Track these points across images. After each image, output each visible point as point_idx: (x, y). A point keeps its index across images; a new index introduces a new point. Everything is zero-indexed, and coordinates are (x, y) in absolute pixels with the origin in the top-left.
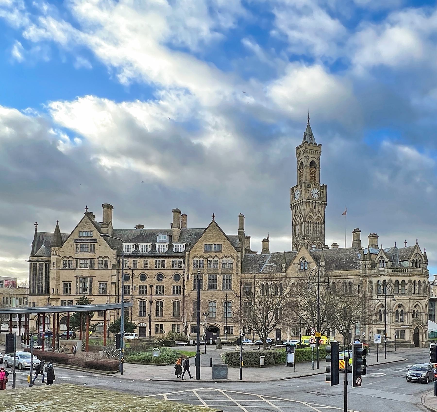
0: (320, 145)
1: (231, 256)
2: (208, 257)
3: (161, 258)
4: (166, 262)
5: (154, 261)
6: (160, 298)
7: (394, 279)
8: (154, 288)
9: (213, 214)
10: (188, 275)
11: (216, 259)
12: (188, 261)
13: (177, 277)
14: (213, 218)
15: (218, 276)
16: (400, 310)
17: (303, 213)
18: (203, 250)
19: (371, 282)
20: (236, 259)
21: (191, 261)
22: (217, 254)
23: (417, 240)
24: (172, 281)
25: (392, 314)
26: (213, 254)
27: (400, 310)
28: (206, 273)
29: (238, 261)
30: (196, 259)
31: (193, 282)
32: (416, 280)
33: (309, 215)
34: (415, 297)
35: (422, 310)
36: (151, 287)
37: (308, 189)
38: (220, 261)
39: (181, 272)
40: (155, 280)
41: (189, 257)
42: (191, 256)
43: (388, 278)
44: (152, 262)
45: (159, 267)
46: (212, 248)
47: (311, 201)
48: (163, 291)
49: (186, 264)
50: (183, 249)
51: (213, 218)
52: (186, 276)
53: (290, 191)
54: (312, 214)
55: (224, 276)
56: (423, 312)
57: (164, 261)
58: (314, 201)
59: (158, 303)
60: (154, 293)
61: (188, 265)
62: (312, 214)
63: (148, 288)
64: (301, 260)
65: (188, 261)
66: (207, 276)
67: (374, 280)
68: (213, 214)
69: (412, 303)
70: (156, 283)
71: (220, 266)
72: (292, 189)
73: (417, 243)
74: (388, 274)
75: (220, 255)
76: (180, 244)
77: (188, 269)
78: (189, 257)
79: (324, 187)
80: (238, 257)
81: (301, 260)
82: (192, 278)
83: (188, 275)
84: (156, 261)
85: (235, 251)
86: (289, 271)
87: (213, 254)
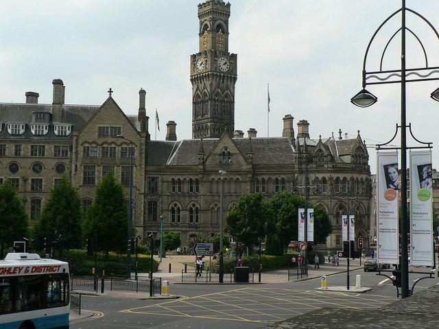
1: (132, 143)
2: (104, 143)
3: (38, 143)
4: (46, 148)
5: (30, 146)
6: (37, 195)
7: (335, 176)
8: (30, 181)
9: (110, 89)
10: (76, 166)
11: (113, 146)
12: (77, 148)
13: (60, 168)
14: (110, 94)
15: (116, 167)
17: (209, 89)
18: (97, 133)
19: (307, 179)
21: (81, 149)
22: (113, 140)
23: (359, 132)
24: (54, 172)
26: (110, 140)
28: (99, 164)
30: (87, 145)
31: (82, 175)
36: (25, 181)
38: (118, 149)
39: (66, 162)
40: (30, 172)
41: (77, 144)
42: (80, 142)
43: (327, 176)
44: (26, 149)
45: (36, 154)
46: (107, 132)
47: (218, 74)
48: (41, 187)
49: (74, 151)
50: (68, 132)
51: (110, 94)
52: (74, 167)
53: (188, 62)
54: (220, 91)
55: (123, 167)
57: (44, 147)
58: (222, 74)
59: (33, 201)
60: (29, 188)
61: (77, 153)
62: (220, 91)
63: (20, 181)
64: (223, 150)
65: (77, 148)
66: (101, 167)
67: (312, 177)
68: (110, 89)
70: (32, 176)
71: (118, 154)
72: (194, 57)
73: (359, 135)
74: (329, 172)
75: (120, 141)
76: (64, 125)
77: (77, 158)
78: (77, 144)
80: (141, 144)
81: (223, 150)
82: (81, 169)
83: (76, 166)
84: (32, 146)
86: (207, 163)
87: (110, 140)
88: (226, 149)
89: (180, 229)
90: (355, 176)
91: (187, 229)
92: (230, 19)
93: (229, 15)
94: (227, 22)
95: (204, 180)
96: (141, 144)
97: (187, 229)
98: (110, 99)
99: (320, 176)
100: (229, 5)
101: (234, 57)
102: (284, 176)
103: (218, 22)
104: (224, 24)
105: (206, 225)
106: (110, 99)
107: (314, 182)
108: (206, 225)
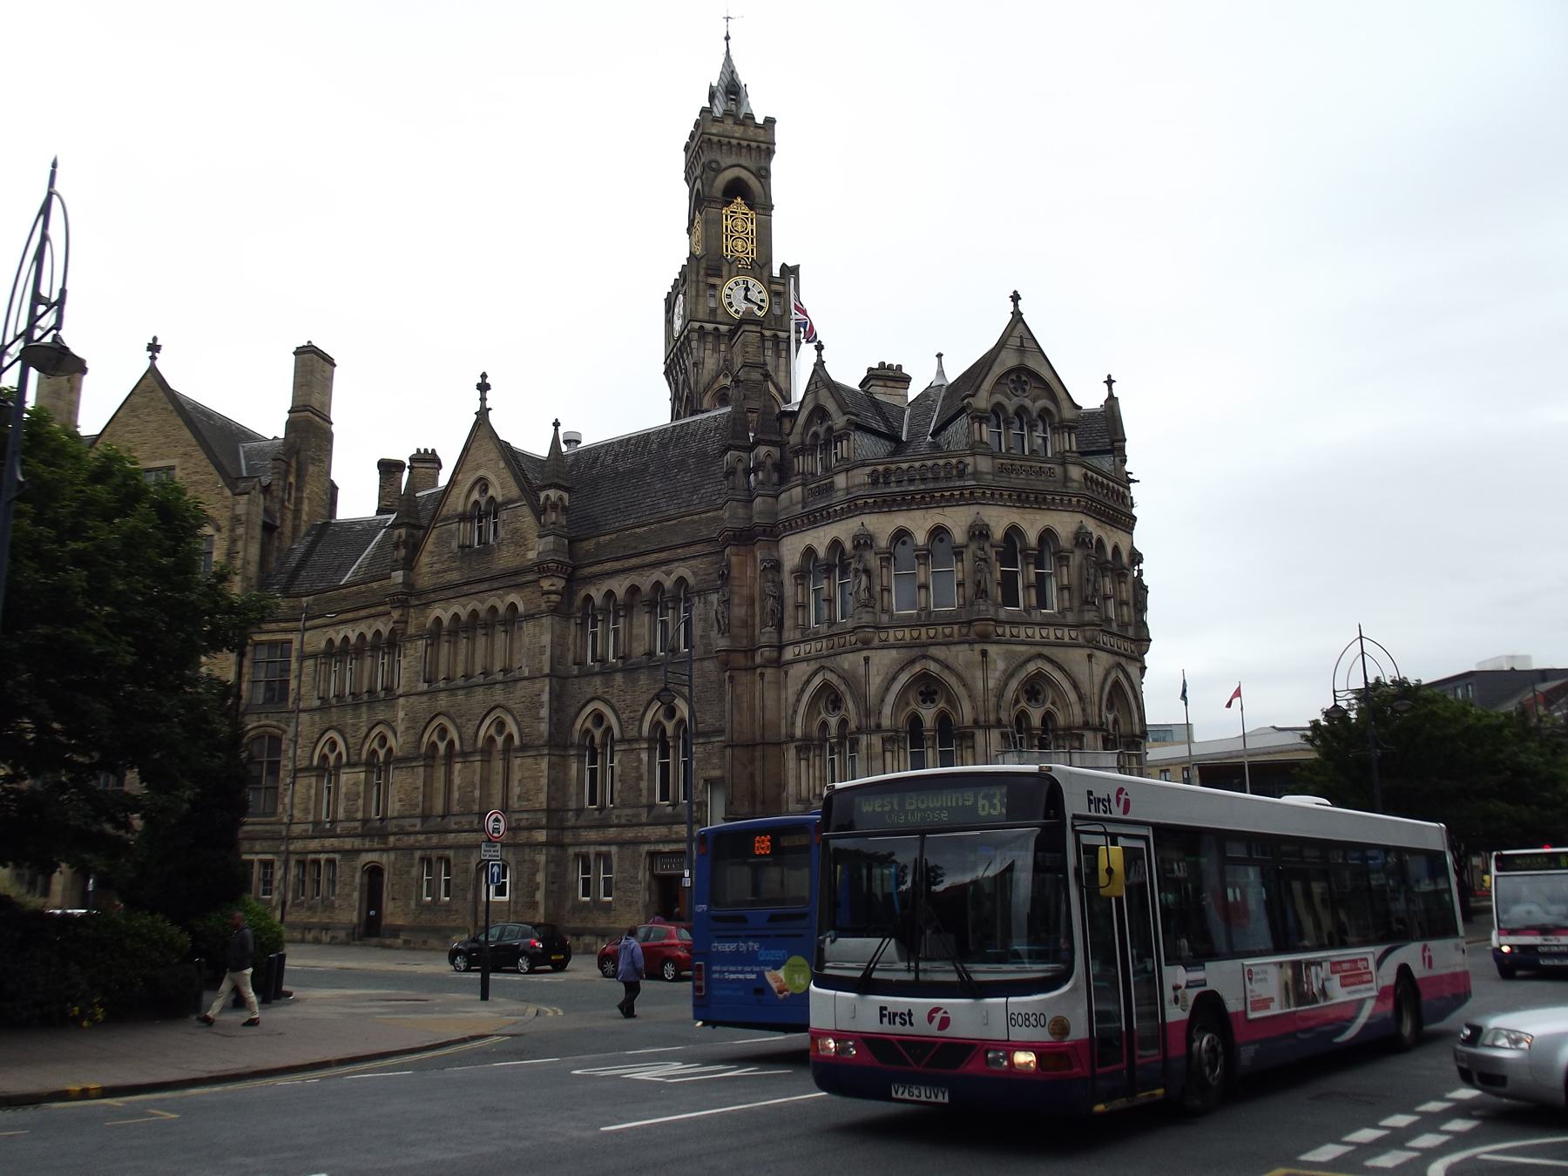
0: (770, 122)
16: (928, 715)
20: (225, 534)
25: (876, 740)
27: (928, 715)
29: (234, 541)
32: (1024, 525)
33: (716, 386)
34: (1022, 632)
35: (1077, 709)
37: (712, 280)
51: (153, 358)
56: (1086, 725)
69: (1001, 665)
79: (790, 272)
80: (236, 520)
81: (475, 496)
85: (228, 492)
88: (485, 490)
89: (335, 842)
90: (999, 519)
91: (357, 843)
92: (776, 165)
93: (770, 152)
94: (764, 175)
95: (411, 630)
96: (236, 520)
97: (357, 843)
98: (153, 372)
99: (820, 538)
100: (770, 122)
101: (790, 272)
102: (682, 570)
103: (729, 175)
104: (753, 182)
105: (406, 822)
106: (153, 372)
107: (801, 574)
108: (406, 822)
